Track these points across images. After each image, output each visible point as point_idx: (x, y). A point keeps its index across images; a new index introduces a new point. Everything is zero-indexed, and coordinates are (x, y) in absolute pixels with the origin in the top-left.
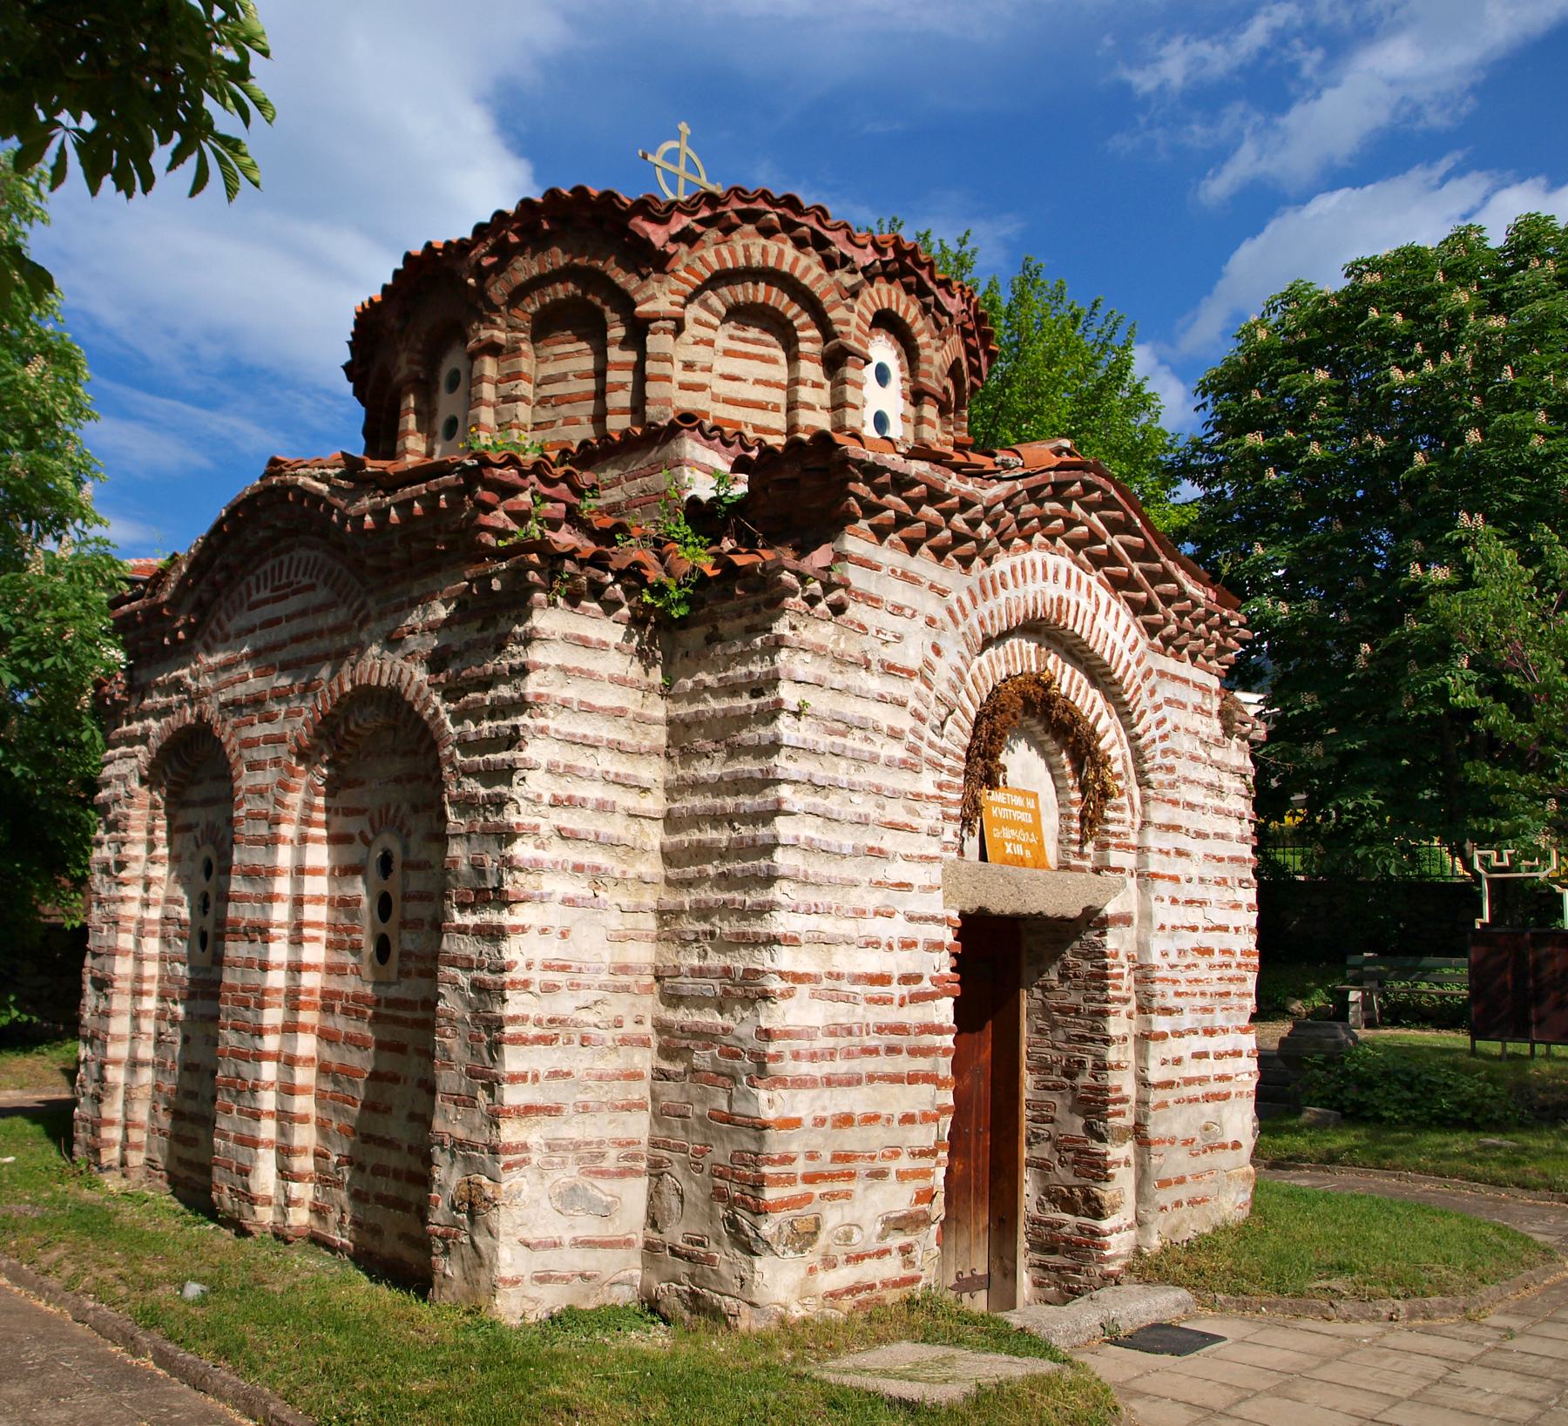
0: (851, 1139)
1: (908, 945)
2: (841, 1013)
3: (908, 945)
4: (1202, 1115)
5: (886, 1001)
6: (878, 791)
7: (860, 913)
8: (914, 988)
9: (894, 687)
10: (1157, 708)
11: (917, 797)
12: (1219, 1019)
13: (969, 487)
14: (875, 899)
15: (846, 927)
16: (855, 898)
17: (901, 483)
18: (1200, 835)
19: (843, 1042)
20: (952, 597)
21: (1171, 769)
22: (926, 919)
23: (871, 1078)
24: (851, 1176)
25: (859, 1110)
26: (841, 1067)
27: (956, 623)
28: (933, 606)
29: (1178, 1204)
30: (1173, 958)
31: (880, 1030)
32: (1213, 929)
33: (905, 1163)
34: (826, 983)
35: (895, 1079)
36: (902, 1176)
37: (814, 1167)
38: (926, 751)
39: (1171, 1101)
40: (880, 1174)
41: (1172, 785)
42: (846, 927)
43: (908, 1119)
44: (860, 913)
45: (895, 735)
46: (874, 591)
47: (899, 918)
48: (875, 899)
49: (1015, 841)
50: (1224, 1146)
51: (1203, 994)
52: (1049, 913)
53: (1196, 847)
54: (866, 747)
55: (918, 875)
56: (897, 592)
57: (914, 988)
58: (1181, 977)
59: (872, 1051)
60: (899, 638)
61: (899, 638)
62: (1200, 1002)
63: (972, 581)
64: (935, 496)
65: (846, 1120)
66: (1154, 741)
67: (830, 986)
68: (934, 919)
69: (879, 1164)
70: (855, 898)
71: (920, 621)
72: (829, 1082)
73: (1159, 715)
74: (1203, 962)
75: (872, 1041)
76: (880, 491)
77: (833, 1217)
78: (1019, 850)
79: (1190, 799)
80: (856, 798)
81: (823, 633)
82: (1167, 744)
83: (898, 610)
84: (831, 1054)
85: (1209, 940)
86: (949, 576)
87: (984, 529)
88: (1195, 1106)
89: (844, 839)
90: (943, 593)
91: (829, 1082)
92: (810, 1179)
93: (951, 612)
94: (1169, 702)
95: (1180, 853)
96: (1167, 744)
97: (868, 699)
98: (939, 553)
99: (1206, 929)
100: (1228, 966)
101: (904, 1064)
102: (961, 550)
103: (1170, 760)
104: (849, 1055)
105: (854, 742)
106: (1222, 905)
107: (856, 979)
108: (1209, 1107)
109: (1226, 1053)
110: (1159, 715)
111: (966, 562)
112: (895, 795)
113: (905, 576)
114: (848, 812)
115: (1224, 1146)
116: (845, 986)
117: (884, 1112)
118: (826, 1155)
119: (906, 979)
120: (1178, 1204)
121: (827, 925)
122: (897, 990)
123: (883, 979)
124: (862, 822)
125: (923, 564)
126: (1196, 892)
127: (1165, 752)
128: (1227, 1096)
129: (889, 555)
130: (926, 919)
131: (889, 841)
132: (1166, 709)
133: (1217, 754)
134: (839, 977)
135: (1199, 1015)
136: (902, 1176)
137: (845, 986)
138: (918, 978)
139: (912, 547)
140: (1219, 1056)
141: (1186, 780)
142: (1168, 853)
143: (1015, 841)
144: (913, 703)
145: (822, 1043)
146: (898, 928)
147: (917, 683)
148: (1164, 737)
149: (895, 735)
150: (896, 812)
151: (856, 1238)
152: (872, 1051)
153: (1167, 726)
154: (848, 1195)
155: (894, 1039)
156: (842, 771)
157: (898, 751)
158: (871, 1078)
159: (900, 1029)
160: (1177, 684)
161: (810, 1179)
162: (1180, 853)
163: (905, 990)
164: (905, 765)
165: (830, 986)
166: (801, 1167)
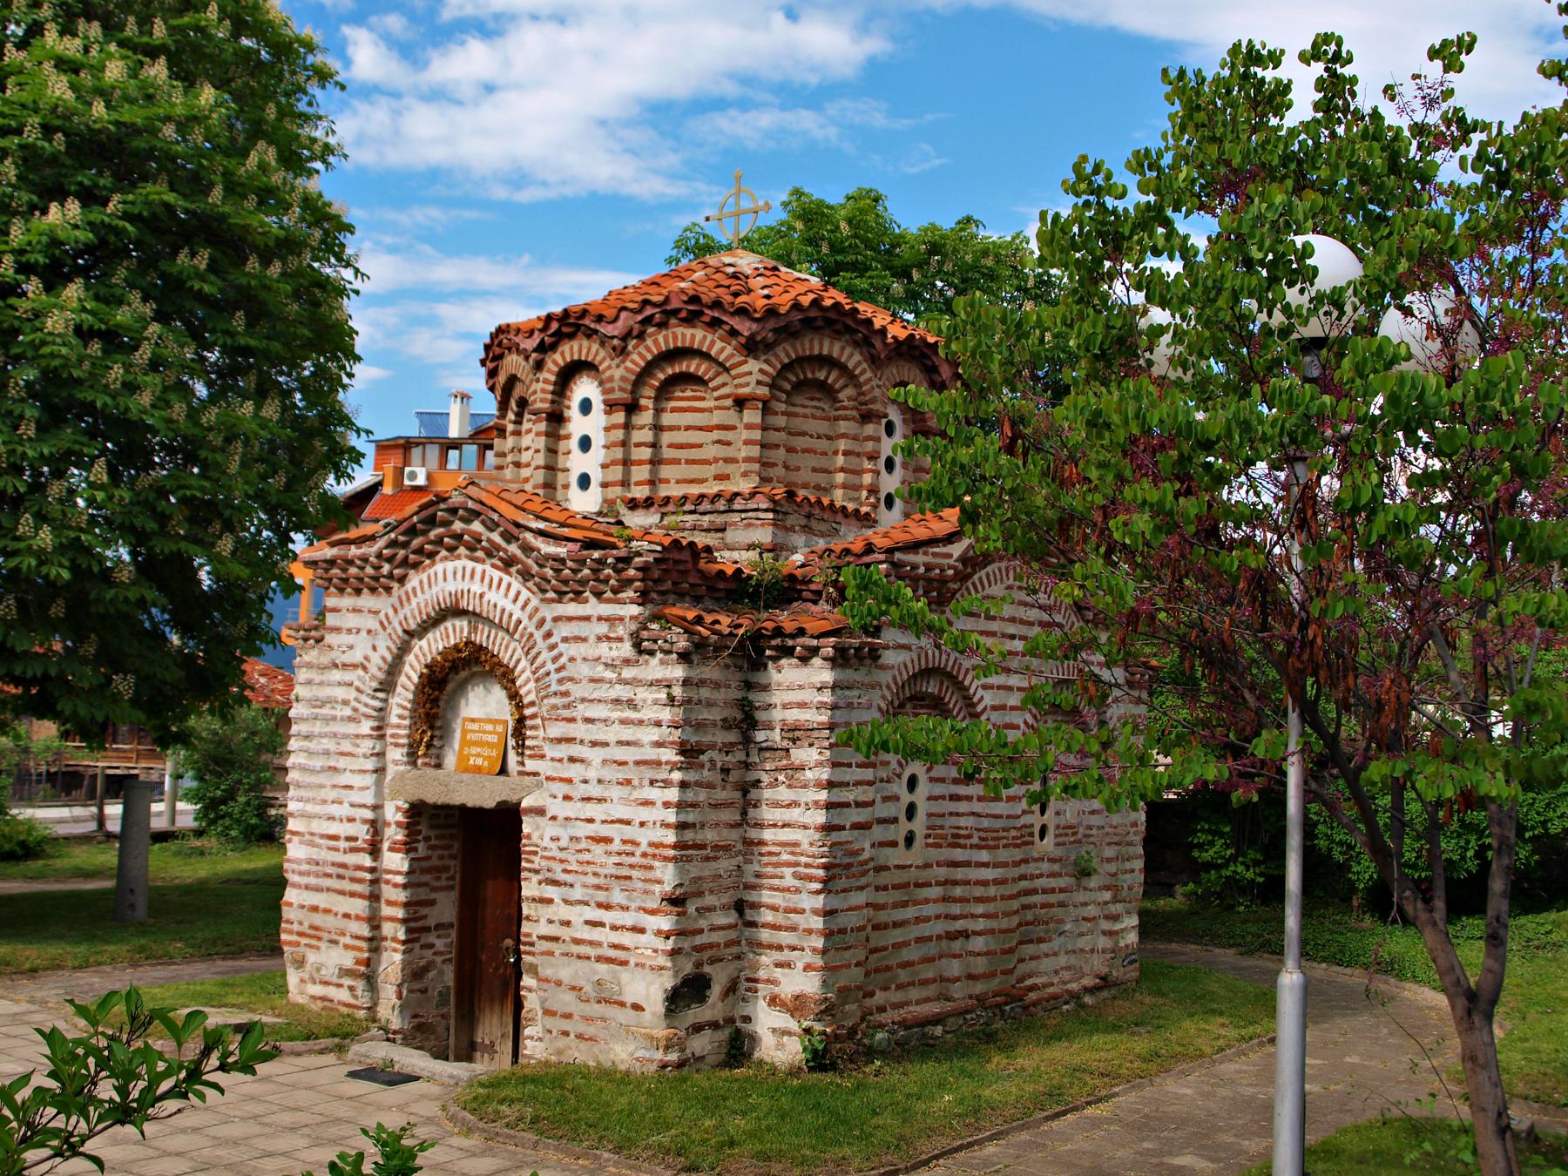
0: (318, 919)
1: (351, 820)
2: (314, 853)
3: (351, 820)
4: (595, 972)
5: (337, 850)
6: (335, 735)
7: (324, 802)
8: (353, 844)
9: (349, 676)
10: (553, 647)
11: (357, 736)
12: (618, 897)
13: (365, 550)
14: (332, 794)
15: (318, 809)
16: (323, 794)
17: (331, 563)
18: (594, 744)
19: (314, 868)
20: (382, 615)
21: (566, 694)
22: (360, 806)
23: (328, 890)
24: (319, 939)
25: (322, 906)
26: (313, 881)
27: (384, 628)
28: (372, 623)
29: (566, 1034)
30: (564, 843)
31: (333, 864)
32: (613, 822)
33: (348, 940)
34: (307, 837)
35: (342, 893)
36: (346, 947)
37: (301, 929)
38: (363, 709)
39: (557, 953)
40: (335, 942)
41: (567, 706)
42: (318, 809)
43: (347, 916)
44: (324, 802)
45: (345, 703)
46: (338, 624)
47: (346, 805)
48: (332, 794)
49: (478, 755)
50: (622, 1004)
51: (595, 874)
52: (470, 805)
53: (595, 755)
54: (333, 712)
55: (357, 781)
56: (351, 621)
57: (353, 844)
58: (571, 858)
59: (329, 876)
60: (351, 647)
61: (351, 647)
62: (592, 880)
63: (394, 600)
64: (351, 562)
65: (315, 909)
66: (548, 674)
67: (310, 839)
68: (364, 806)
69: (335, 937)
70: (323, 794)
71: (364, 633)
72: (307, 887)
73: (555, 652)
74: (599, 849)
75: (330, 870)
76: (327, 571)
77: (312, 957)
78: (479, 761)
79: (588, 715)
80: (324, 741)
81: (311, 655)
82: (563, 674)
83: (349, 631)
84: (308, 874)
85: (605, 830)
86: (381, 603)
87: (386, 568)
88: (586, 962)
89: (318, 763)
90: (377, 613)
91: (307, 887)
92: (300, 934)
93: (381, 623)
94: (565, 640)
95: (572, 760)
96: (563, 674)
97: (335, 685)
98: (373, 590)
99: (604, 822)
100: (633, 854)
101: (347, 885)
102: (377, 585)
103: (568, 686)
104: (317, 876)
105: (326, 711)
106: (626, 801)
107: (323, 836)
108: (603, 968)
109: (623, 927)
110: (555, 652)
111: (388, 590)
112: (345, 736)
113: (354, 610)
114: (320, 748)
115: (622, 1004)
116: (318, 840)
117: (335, 909)
118: (306, 924)
119: (348, 839)
120: (566, 1034)
121: (310, 808)
122: (343, 844)
123: (335, 838)
124: (327, 753)
125: (366, 601)
126: (594, 790)
127: (560, 681)
128: (624, 963)
129: (347, 601)
130: (360, 806)
131: (342, 763)
132: (562, 647)
133: (628, 673)
134: (312, 834)
135: (591, 891)
136: (346, 947)
137: (318, 840)
138: (355, 839)
139: (358, 592)
140: (614, 928)
141: (583, 700)
142: (560, 760)
143: (478, 755)
144: (356, 683)
145: (305, 867)
146: (345, 810)
147: (360, 672)
148: (558, 670)
149: (345, 703)
150: (346, 746)
151: (323, 972)
152: (329, 876)
153: (563, 660)
154: (318, 948)
155: (341, 871)
156: (318, 728)
157: (348, 712)
158: (328, 890)
159: (344, 866)
160: (574, 623)
161: (300, 934)
162: (572, 760)
163: (347, 845)
164: (351, 719)
165: (310, 839)
166: (296, 927)
